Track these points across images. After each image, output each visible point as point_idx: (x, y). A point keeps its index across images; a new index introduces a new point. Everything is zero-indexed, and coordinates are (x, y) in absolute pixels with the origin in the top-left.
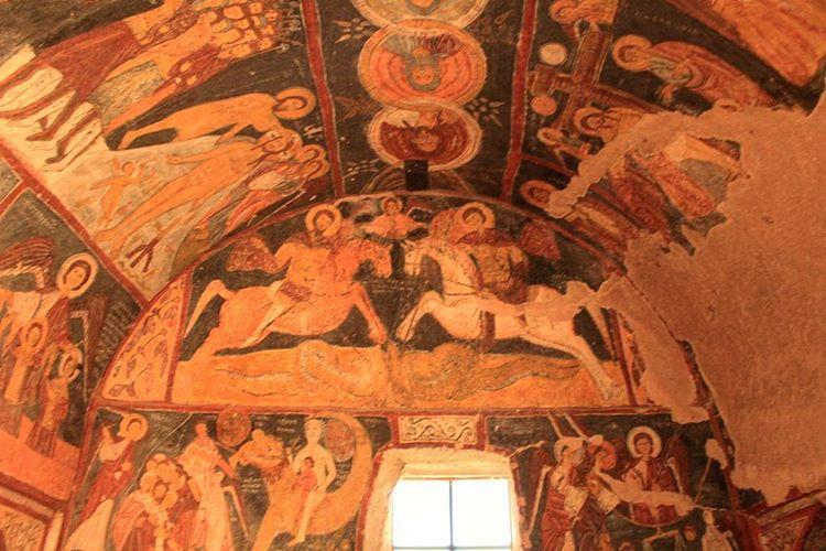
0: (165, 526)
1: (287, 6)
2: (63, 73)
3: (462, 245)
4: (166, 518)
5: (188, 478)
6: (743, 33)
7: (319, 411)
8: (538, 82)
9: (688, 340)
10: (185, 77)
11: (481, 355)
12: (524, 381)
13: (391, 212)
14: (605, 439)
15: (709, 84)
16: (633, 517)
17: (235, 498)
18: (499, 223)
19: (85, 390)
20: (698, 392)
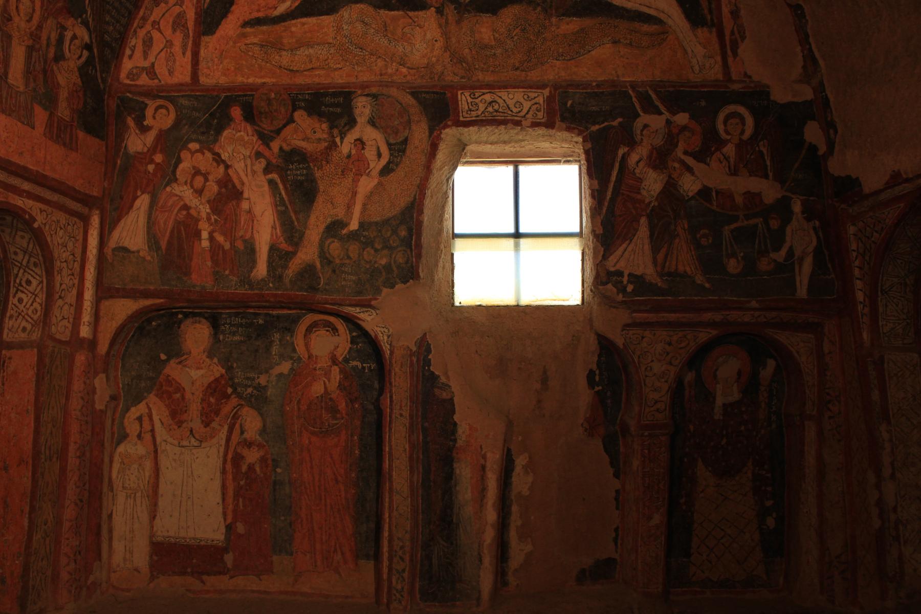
0: (209, 219)
4: (208, 210)
5: (227, 167)
7: (367, 87)
9: (801, 3)
11: (554, 20)
12: (604, 51)
14: (692, 117)
16: (715, 203)
17: (281, 186)
19: (98, 74)
20: (804, 67)
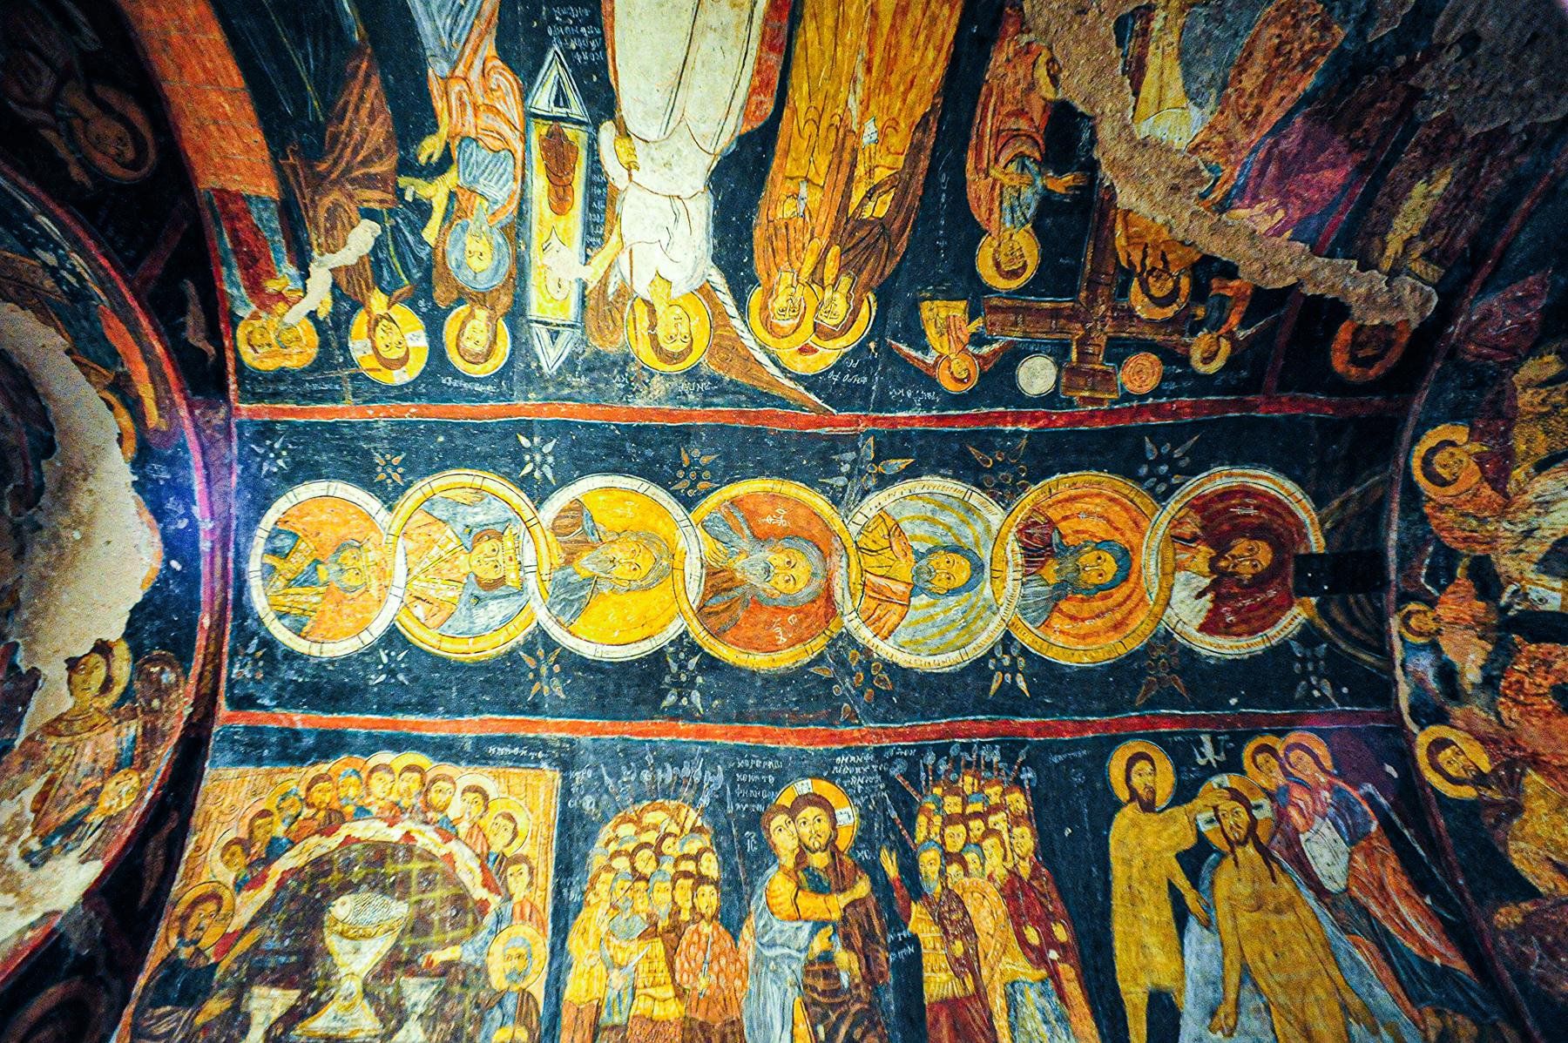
1: (957, 760)
3: (1511, 487)
6: (919, 112)
8: (1092, 389)
10: (1049, 941)
13: (1433, 626)
15: (1023, 124)
18: (1455, 415)
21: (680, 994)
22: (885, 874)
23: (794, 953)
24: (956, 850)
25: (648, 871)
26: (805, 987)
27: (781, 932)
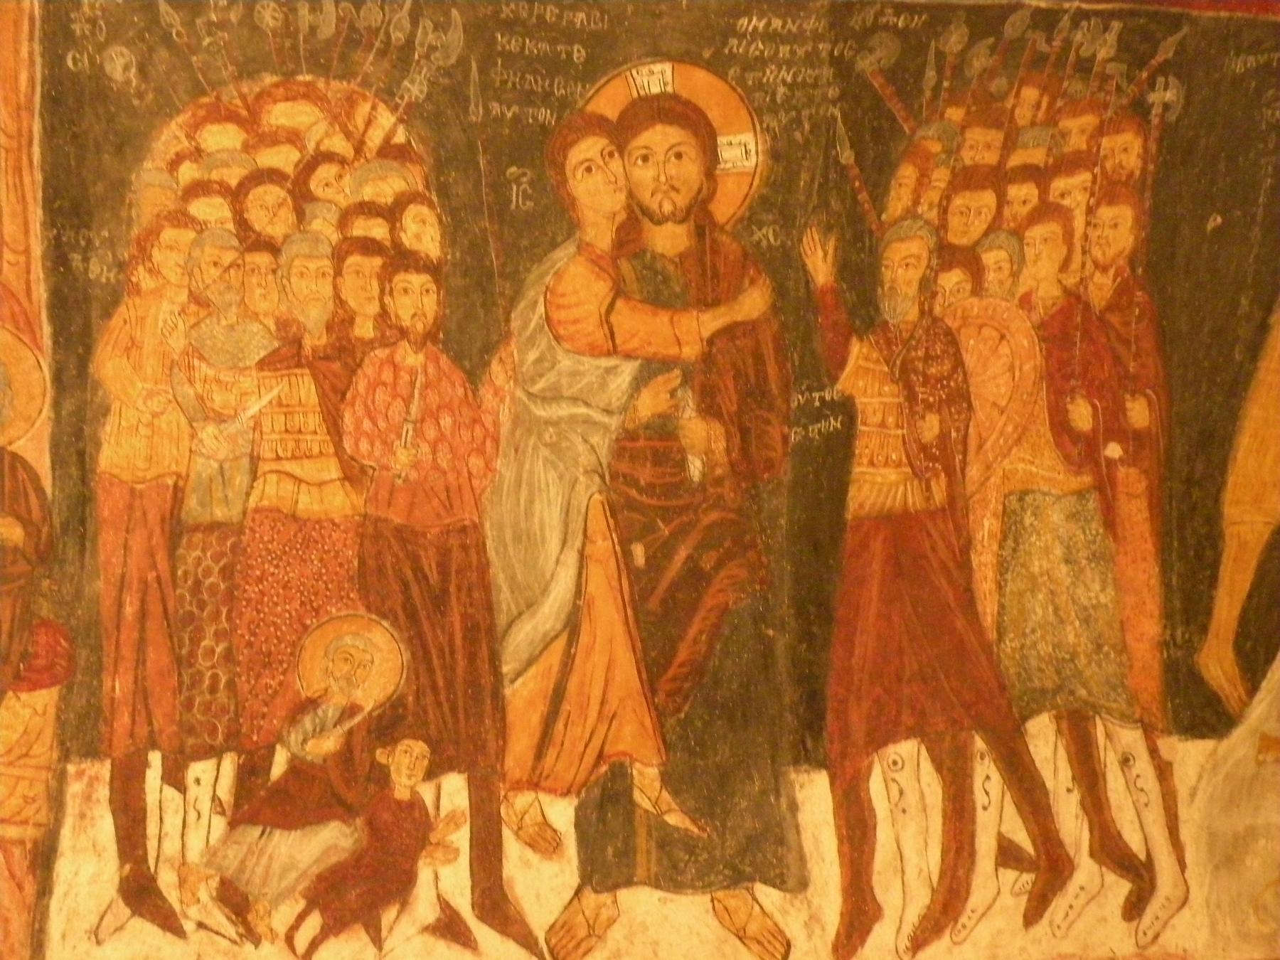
2: (910, 733)
10: (1113, 425)
21: (353, 474)
22: (808, 280)
23: (597, 416)
24: (964, 241)
25: (277, 230)
26: (614, 477)
27: (574, 374)
